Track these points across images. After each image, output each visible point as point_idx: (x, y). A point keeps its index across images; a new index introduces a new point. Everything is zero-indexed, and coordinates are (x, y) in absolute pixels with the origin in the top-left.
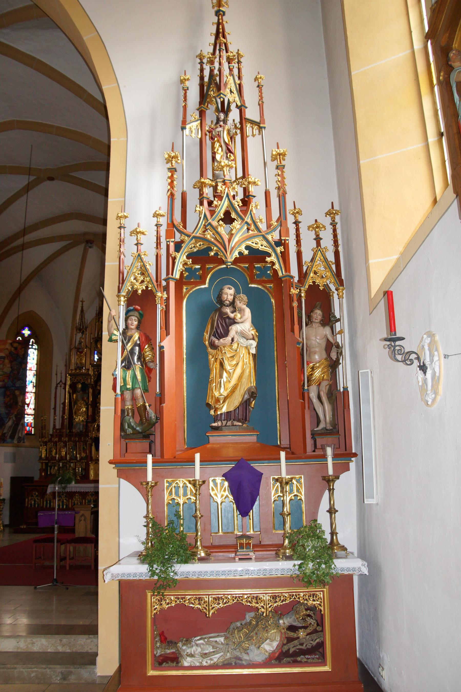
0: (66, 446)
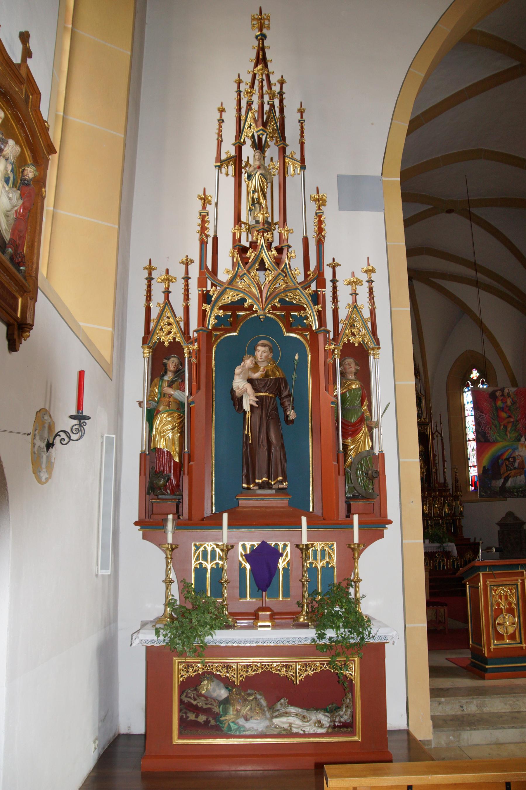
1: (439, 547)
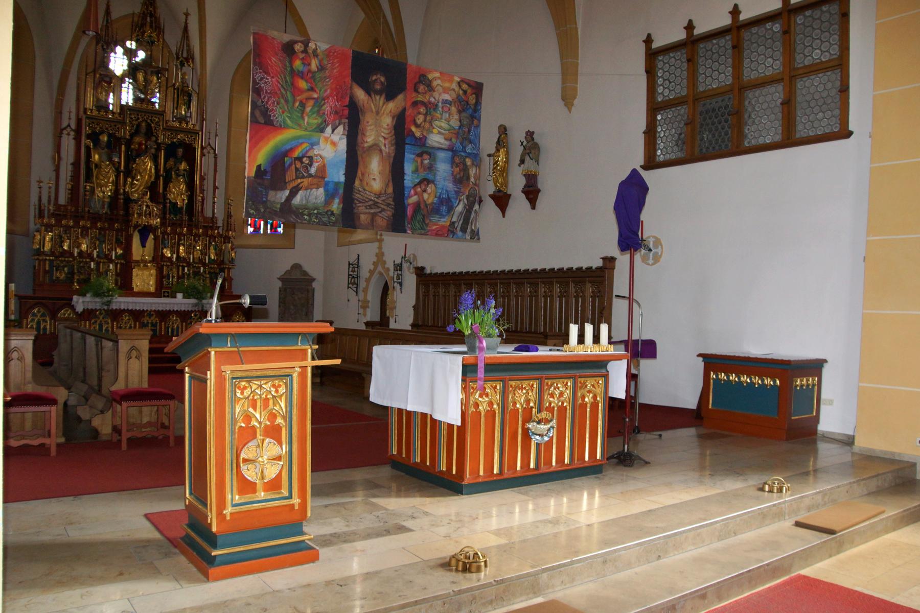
1: (196, 305)
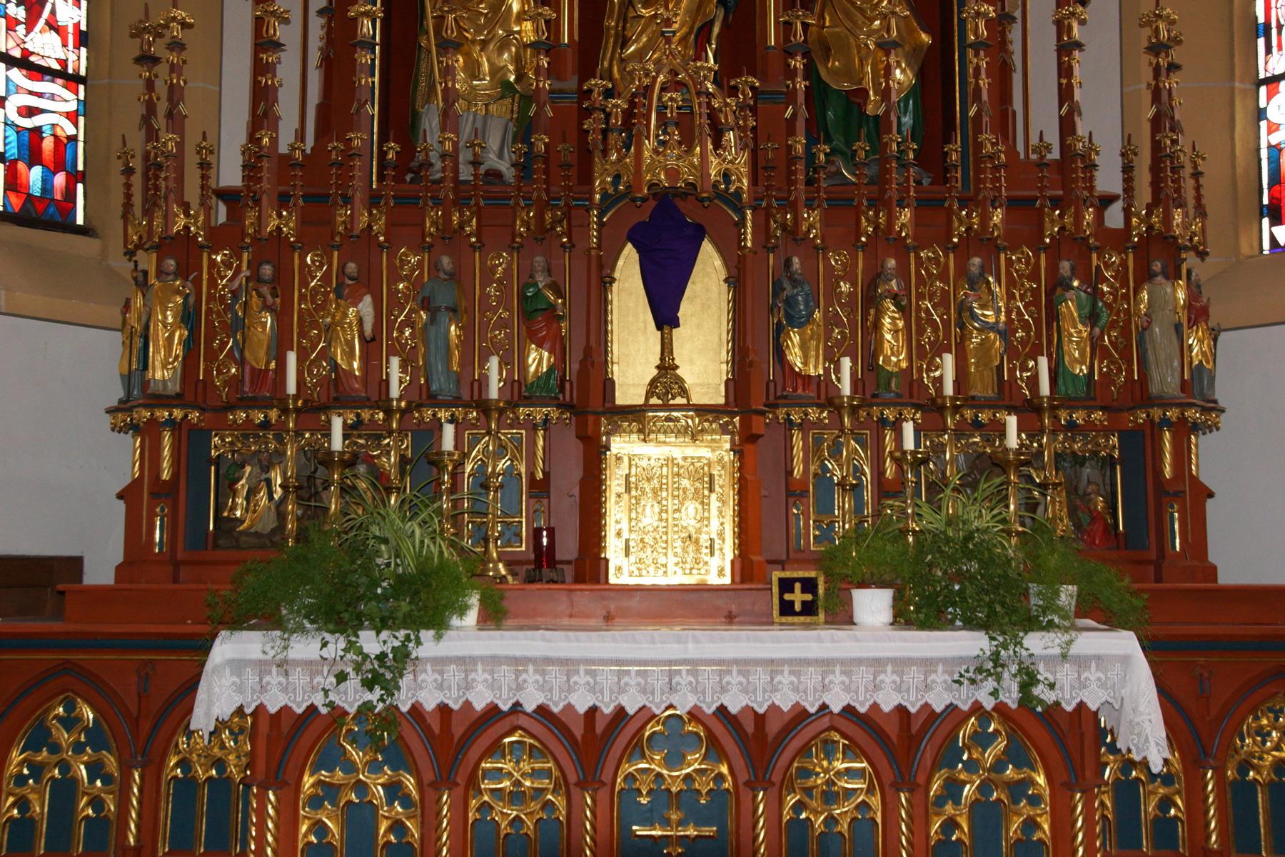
0: (367, 283)
1: (992, 666)
